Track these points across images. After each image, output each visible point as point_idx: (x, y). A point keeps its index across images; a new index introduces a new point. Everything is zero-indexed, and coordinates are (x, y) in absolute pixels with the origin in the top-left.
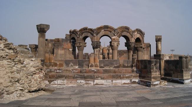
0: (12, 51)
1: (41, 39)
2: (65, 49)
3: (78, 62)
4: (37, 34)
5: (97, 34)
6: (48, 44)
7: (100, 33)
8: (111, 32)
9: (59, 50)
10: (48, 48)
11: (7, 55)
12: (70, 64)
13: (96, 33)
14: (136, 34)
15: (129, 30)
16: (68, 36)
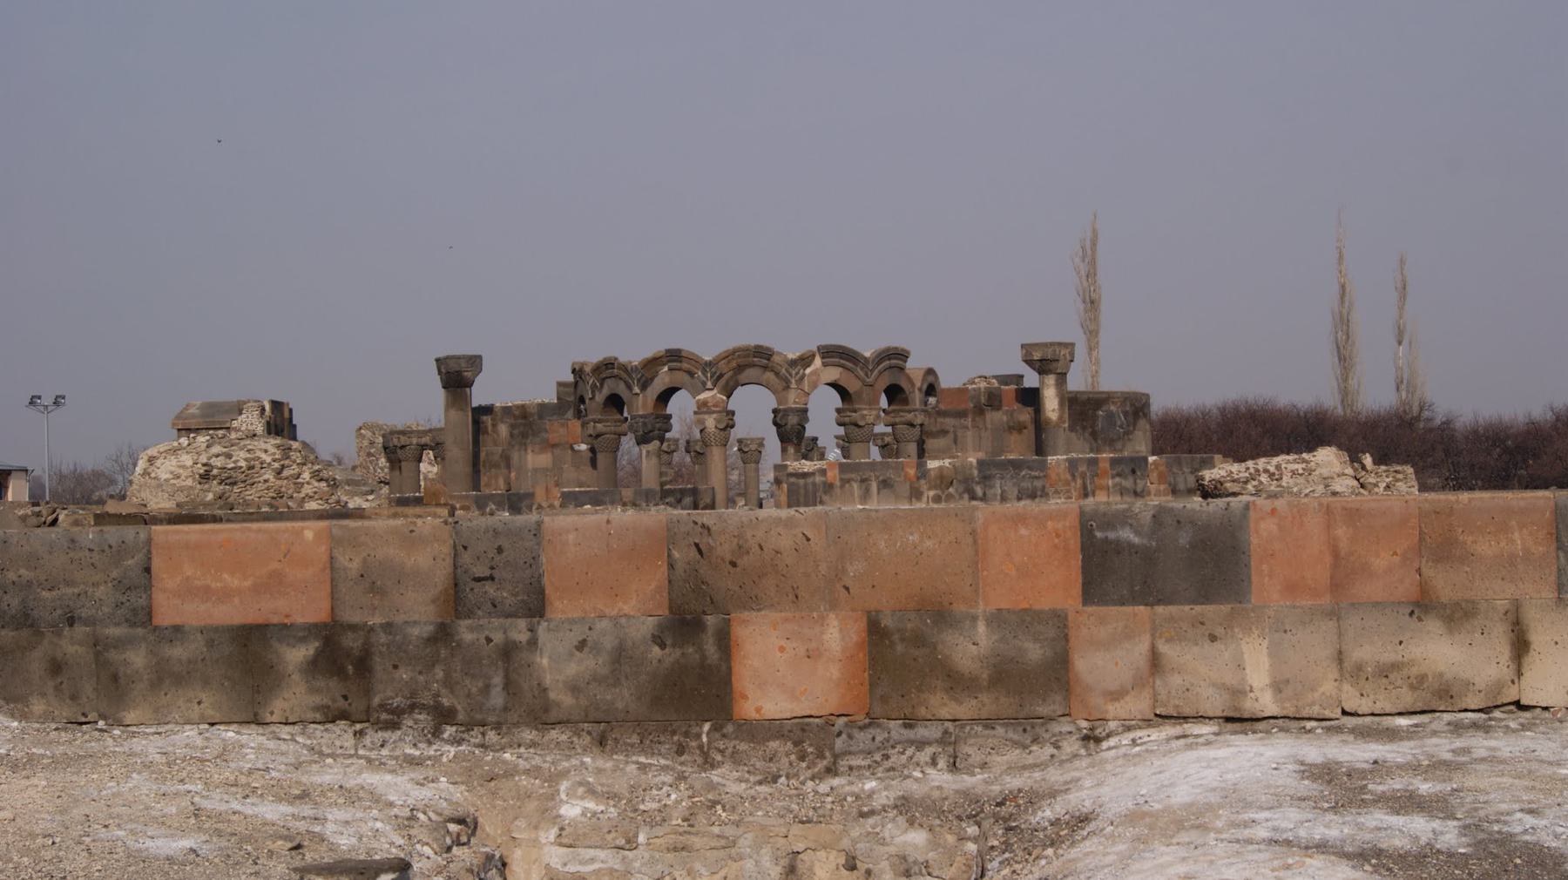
0: (323, 484)
1: (453, 413)
2: (554, 446)
3: (509, 499)
4: (439, 395)
5: (644, 387)
6: (494, 425)
7: (657, 381)
8: (691, 374)
9: (529, 451)
10: (495, 444)
11: (315, 493)
12: (487, 506)
13: (639, 380)
14: (814, 373)
15: (776, 358)
16: (566, 389)
